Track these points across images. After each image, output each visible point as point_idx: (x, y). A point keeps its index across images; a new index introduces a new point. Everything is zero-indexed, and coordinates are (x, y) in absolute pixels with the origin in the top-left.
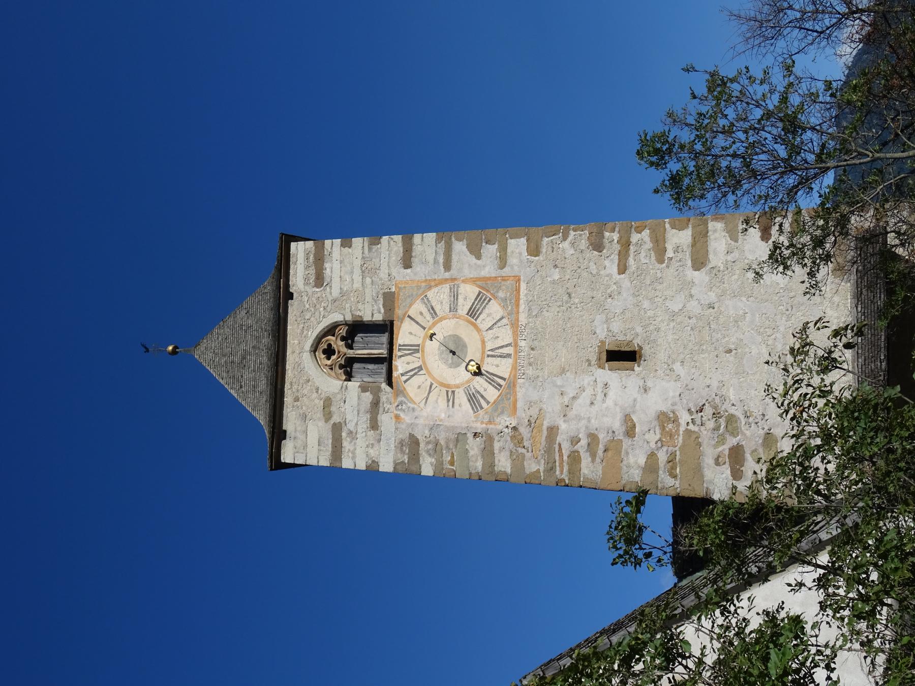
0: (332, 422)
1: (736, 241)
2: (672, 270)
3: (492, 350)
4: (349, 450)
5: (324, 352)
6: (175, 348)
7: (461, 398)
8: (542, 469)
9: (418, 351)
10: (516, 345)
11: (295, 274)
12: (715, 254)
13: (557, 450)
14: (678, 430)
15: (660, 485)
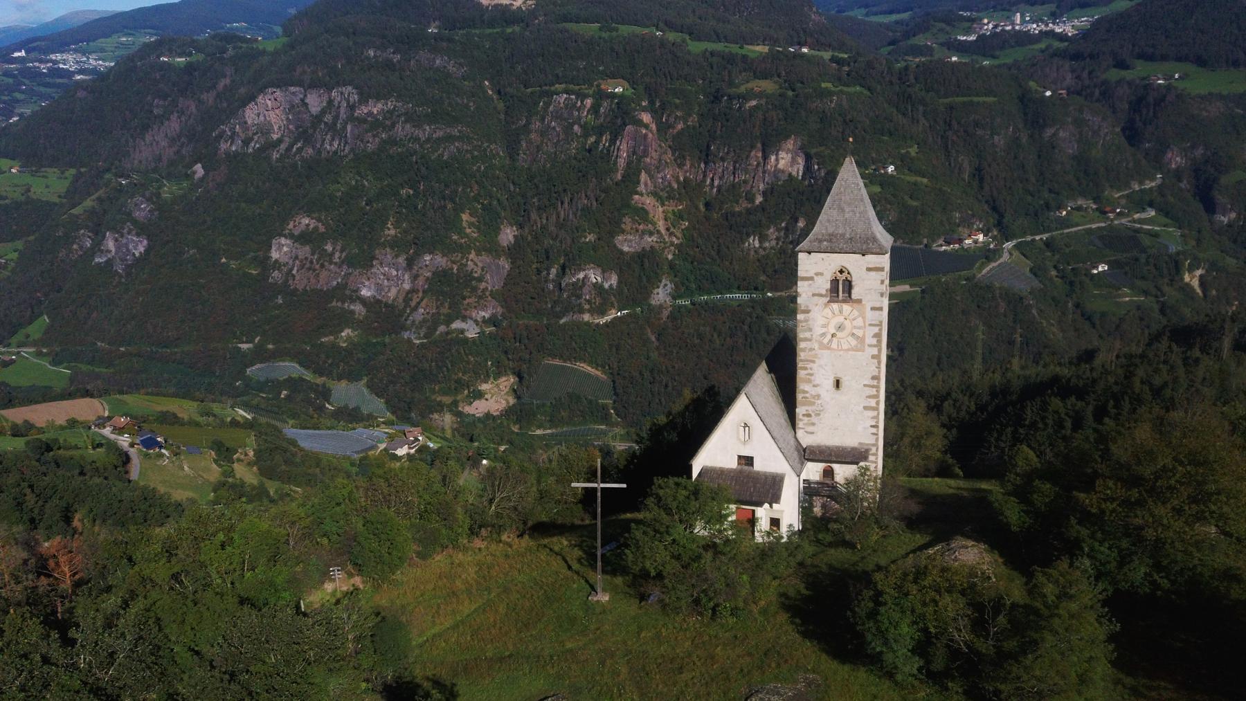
7: (824, 330)
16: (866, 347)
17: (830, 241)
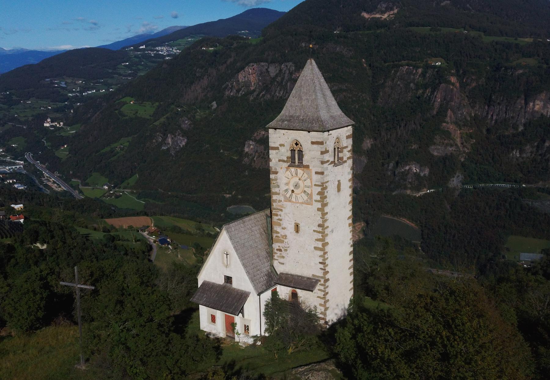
0: (279, 147)
7: (287, 187)
8: (274, 207)
16: (314, 201)
17: (289, 121)
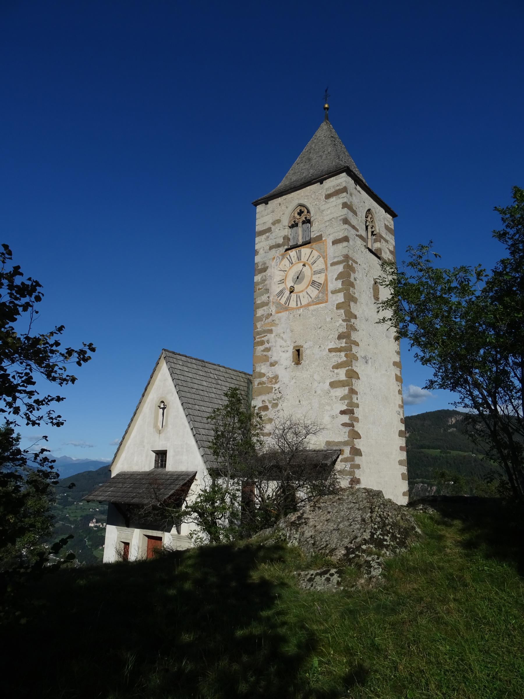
1: (340, 400)
2: (329, 373)
3: (299, 296)
4: (262, 239)
5: (301, 210)
6: (327, 109)
7: (282, 286)
8: (258, 330)
9: (298, 260)
10: (301, 307)
11: (332, 181)
12: (336, 391)
13: (265, 335)
14: (272, 384)
15: (255, 380)
16: (330, 295)
